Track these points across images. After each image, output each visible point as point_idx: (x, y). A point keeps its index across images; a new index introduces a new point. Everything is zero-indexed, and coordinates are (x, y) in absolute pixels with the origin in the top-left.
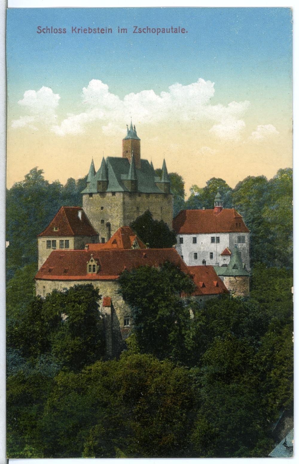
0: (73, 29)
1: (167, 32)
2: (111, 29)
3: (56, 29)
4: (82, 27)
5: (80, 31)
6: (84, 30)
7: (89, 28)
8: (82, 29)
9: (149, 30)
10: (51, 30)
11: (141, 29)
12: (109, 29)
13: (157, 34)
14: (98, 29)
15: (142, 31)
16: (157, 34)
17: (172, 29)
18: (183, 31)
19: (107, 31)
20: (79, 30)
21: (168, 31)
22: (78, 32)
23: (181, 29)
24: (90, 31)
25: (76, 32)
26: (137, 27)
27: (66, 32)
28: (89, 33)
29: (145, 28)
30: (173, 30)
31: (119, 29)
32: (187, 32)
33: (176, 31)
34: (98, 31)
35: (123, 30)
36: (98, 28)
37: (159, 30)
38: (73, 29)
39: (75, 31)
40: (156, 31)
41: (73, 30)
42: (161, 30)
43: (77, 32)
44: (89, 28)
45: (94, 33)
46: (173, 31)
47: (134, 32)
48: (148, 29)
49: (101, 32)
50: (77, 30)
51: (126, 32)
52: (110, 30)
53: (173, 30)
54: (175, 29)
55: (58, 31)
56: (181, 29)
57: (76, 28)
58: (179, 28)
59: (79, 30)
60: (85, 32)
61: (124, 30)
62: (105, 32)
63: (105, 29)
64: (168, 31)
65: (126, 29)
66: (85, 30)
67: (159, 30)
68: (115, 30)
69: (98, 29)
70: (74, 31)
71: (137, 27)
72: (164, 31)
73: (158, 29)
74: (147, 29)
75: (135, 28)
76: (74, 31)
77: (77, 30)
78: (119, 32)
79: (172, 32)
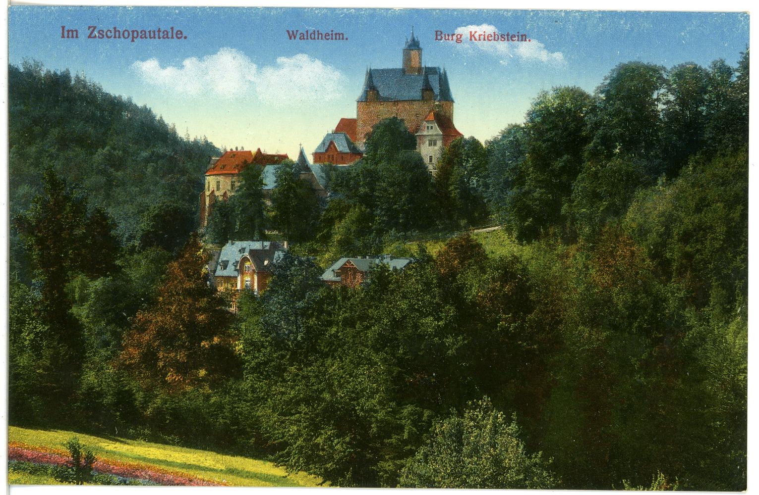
1: (150, 38)
3: (127, 31)
4: (484, 32)
6: (488, 37)
8: (484, 35)
13: (133, 41)
14: (508, 35)
18: (179, 36)
21: (152, 35)
23: (175, 32)
24: (496, 39)
25: (476, 40)
28: (494, 40)
30: (161, 35)
32: (185, 38)
33: (166, 35)
34: (508, 38)
35: (70, 33)
39: (475, 38)
40: (131, 36)
45: (501, 40)
48: (115, 32)
50: (477, 36)
51: (77, 37)
52: (524, 37)
53: (161, 35)
56: (175, 32)
57: (475, 32)
58: (307, 33)
60: (327, 37)
62: (516, 38)
64: (152, 35)
65: (77, 31)
66: (327, 35)
67: (135, 35)
70: (473, 39)
74: (113, 31)
76: (473, 39)
77: (477, 38)
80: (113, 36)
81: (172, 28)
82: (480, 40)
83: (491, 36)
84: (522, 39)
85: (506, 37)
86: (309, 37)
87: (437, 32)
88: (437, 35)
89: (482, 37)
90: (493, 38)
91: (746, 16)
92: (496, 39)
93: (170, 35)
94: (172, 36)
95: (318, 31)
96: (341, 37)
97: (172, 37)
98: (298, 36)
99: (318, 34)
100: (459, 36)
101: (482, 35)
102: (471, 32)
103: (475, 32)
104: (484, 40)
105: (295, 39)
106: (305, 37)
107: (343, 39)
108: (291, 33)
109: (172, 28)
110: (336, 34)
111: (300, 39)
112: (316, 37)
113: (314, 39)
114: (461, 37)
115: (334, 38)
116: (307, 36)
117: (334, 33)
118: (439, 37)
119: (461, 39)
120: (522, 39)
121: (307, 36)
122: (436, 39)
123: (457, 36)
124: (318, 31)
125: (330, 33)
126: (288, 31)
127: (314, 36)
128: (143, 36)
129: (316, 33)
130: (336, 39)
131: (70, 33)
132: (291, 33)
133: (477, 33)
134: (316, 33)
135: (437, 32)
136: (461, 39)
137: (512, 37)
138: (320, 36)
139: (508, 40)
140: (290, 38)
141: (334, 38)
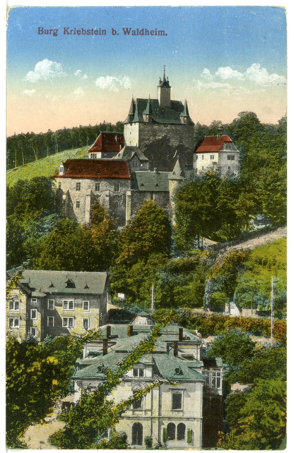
0: (66, 29)
2: (105, 31)
4: (75, 28)
5: (73, 32)
7: (82, 29)
8: (75, 31)
12: (103, 31)
15: (87, 32)
20: (71, 31)
22: (71, 34)
24: (84, 32)
25: (68, 34)
28: (83, 34)
36: (92, 29)
37: (142, 33)
38: (66, 29)
44: (82, 29)
50: (69, 31)
57: (68, 28)
63: (99, 30)
69: (92, 30)
70: (66, 33)
80: (155, 34)
81: (138, 29)
82: (71, 34)
83: (154, 32)
84: (146, 33)
85: (91, 32)
86: (139, 33)
87: (39, 28)
88: (39, 31)
89: (73, 32)
90: (81, 33)
92: (84, 32)
93: (136, 33)
95: (146, 29)
96: (163, 34)
97: (138, 34)
98: (131, 33)
99: (146, 32)
100: (55, 31)
101: (73, 30)
102: (65, 28)
103: (68, 28)
104: (75, 34)
105: (129, 33)
106: (136, 33)
107: (164, 35)
108: (125, 30)
109: (138, 29)
110: (159, 32)
111: (133, 34)
112: (144, 34)
113: (143, 34)
114: (56, 32)
115: (158, 34)
116: (138, 32)
117: (157, 31)
120: (146, 33)
121: (138, 32)
122: (39, 33)
123: (54, 32)
124: (146, 29)
125: (155, 30)
126: (124, 29)
127: (143, 33)
128: (134, 34)
129: (144, 31)
130: (159, 35)
131: (160, 32)
132: (125, 30)
133: (69, 29)
134: (144, 31)
135: (39, 28)
136: (57, 33)
138: (147, 32)
139: (93, 34)
140: (125, 33)
141: (158, 34)
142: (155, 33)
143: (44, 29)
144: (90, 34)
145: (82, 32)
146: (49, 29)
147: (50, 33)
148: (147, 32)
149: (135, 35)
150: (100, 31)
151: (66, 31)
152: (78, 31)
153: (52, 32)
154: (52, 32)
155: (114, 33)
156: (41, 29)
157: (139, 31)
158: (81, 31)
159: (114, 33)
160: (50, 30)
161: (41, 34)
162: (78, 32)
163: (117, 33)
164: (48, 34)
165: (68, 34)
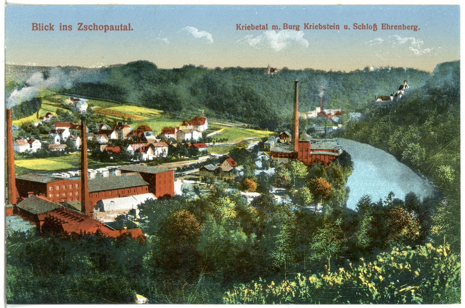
0: (306, 25)
2: (338, 26)
4: (313, 24)
6: (315, 27)
9: (388, 27)
10: (266, 27)
11: (87, 26)
12: (336, 26)
14: (328, 25)
16: (105, 32)
17: (121, 26)
19: (335, 28)
22: (310, 28)
26: (82, 24)
27: (71, 29)
28: (320, 28)
29: (47, 24)
31: (61, 26)
36: (328, 24)
37: (107, 28)
38: (306, 25)
41: (305, 26)
42: (110, 28)
43: (241, 28)
45: (324, 29)
46: (123, 29)
47: (79, 29)
49: (330, 28)
54: (263, 26)
55: (88, 28)
57: (308, 24)
59: (310, 26)
61: (64, 28)
68: (57, 28)
71: (82, 24)
72: (112, 28)
73: (105, 26)
75: (80, 25)
77: (309, 28)
78: (61, 30)
79: (122, 30)
85: (327, 27)
91: (455, 10)
94: (43, 29)
100: (297, 27)
114: (298, 27)
118: (286, 28)
119: (299, 28)
135: (284, 24)
136: (299, 28)
137: (330, 27)
139: (328, 29)
142: (333, 27)
143: (288, 25)
144: (326, 28)
145: (252, 28)
146: (293, 25)
147: (294, 29)
148: (96, 27)
149: (127, 30)
150: (334, 26)
151: (306, 26)
152: (249, 26)
153: (295, 28)
154: (295, 28)
155: (346, 27)
156: (285, 25)
157: (369, 26)
158: (93, 26)
159: (346, 27)
160: (294, 26)
161: (35, 30)
162: (248, 28)
163: (279, 28)
164: (118, 30)
165: (308, 28)
